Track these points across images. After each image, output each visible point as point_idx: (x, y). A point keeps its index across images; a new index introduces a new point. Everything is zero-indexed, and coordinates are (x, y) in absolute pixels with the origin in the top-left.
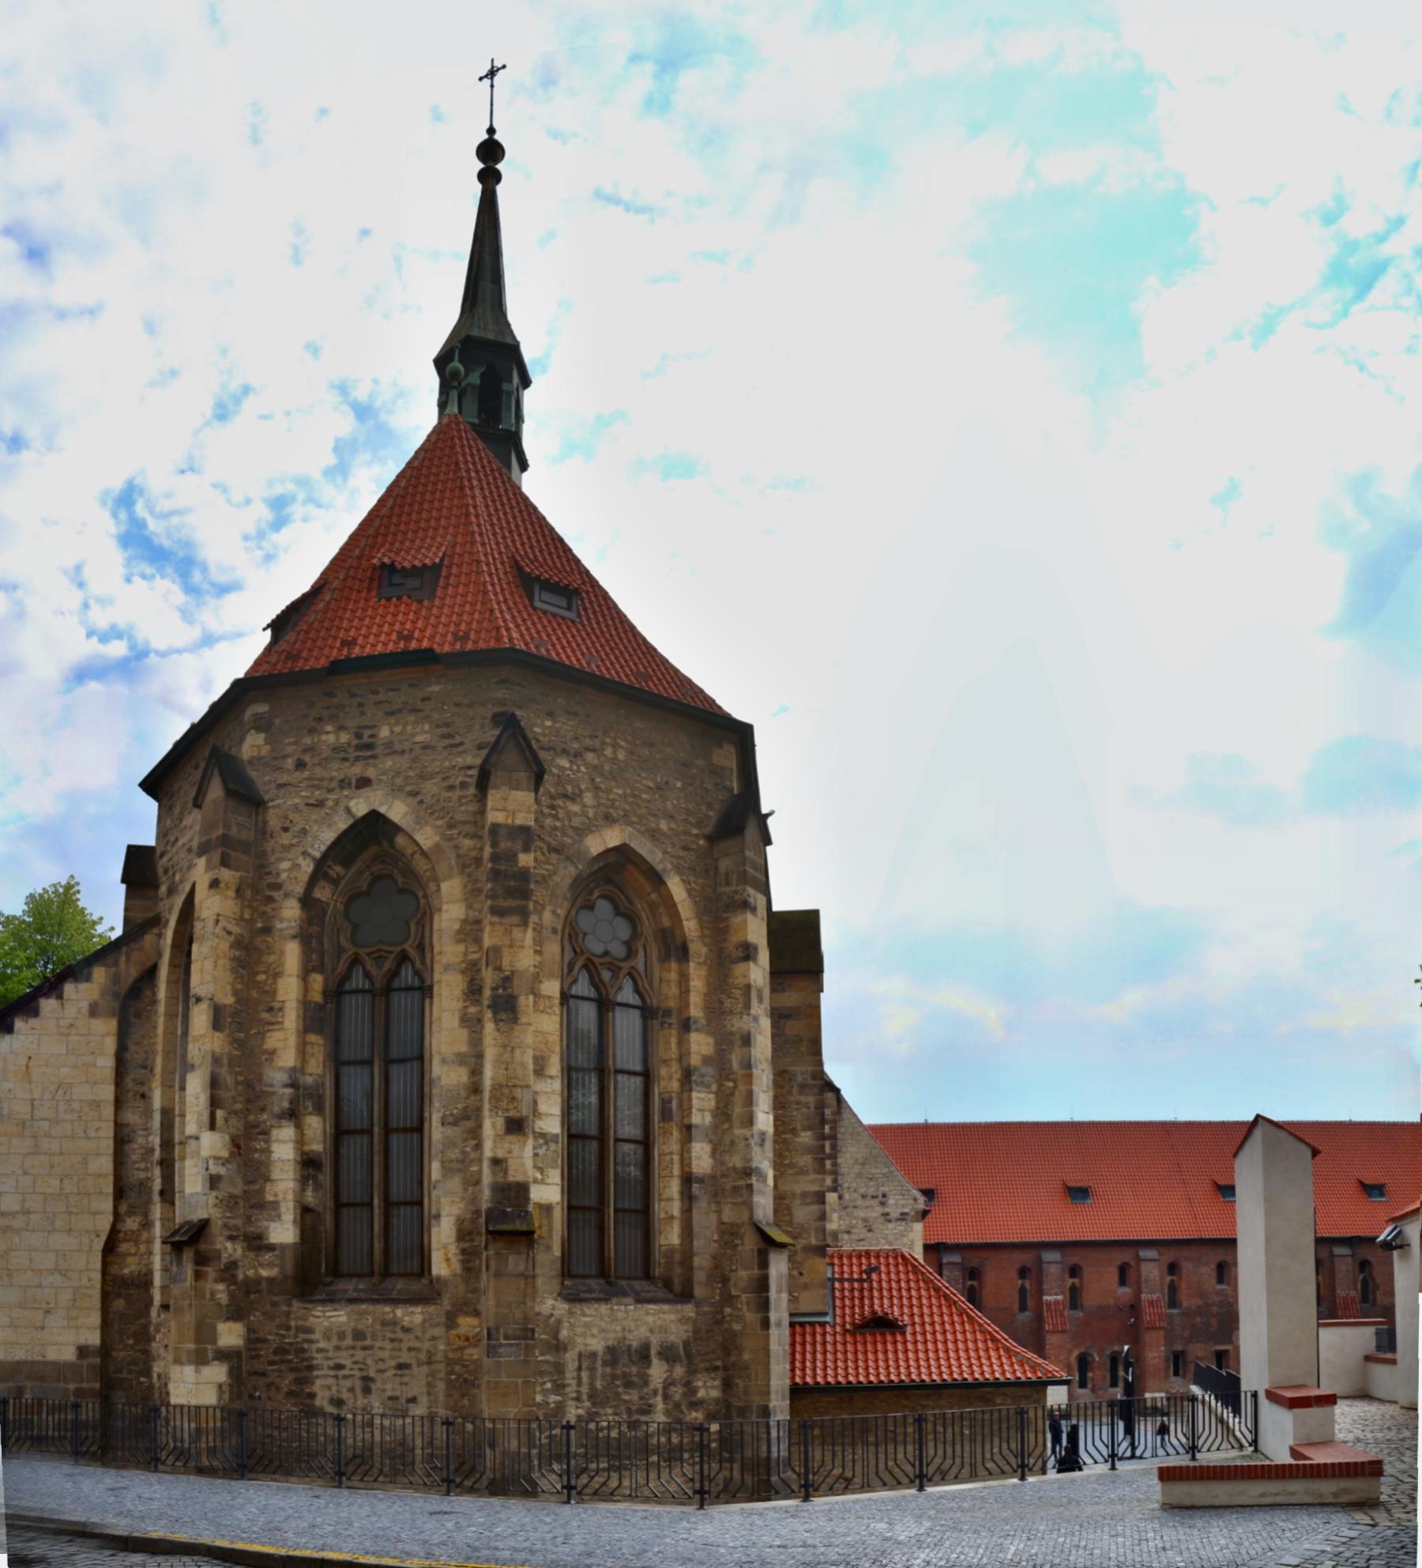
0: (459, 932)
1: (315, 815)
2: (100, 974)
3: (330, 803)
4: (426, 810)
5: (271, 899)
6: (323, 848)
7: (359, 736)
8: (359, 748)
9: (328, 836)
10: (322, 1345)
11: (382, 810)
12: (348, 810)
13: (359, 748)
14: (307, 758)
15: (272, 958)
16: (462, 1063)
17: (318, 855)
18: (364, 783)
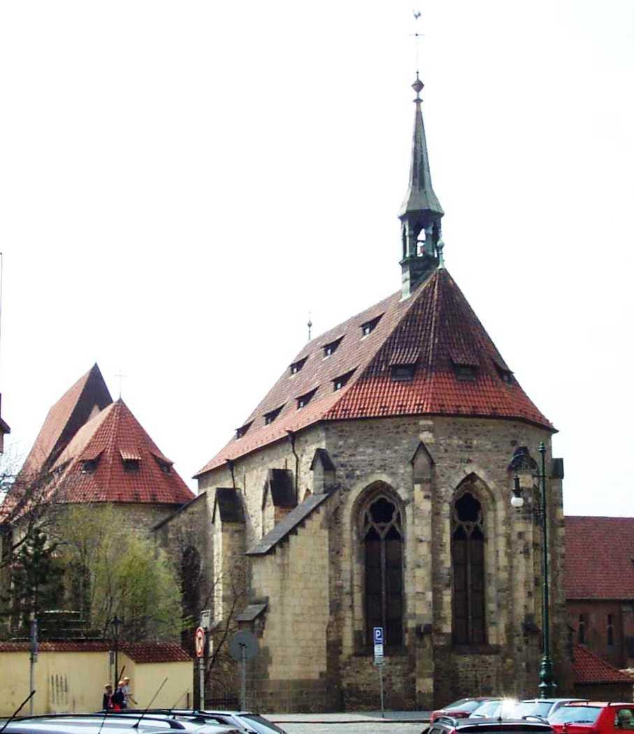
0: (504, 521)
1: (453, 471)
2: (322, 510)
3: (458, 467)
4: (492, 475)
5: (439, 502)
6: (457, 484)
7: (466, 442)
8: (466, 447)
9: (458, 481)
10: (462, 669)
11: (476, 472)
12: (464, 471)
13: (466, 447)
15: (441, 526)
16: (507, 571)
17: (455, 487)
18: (469, 461)
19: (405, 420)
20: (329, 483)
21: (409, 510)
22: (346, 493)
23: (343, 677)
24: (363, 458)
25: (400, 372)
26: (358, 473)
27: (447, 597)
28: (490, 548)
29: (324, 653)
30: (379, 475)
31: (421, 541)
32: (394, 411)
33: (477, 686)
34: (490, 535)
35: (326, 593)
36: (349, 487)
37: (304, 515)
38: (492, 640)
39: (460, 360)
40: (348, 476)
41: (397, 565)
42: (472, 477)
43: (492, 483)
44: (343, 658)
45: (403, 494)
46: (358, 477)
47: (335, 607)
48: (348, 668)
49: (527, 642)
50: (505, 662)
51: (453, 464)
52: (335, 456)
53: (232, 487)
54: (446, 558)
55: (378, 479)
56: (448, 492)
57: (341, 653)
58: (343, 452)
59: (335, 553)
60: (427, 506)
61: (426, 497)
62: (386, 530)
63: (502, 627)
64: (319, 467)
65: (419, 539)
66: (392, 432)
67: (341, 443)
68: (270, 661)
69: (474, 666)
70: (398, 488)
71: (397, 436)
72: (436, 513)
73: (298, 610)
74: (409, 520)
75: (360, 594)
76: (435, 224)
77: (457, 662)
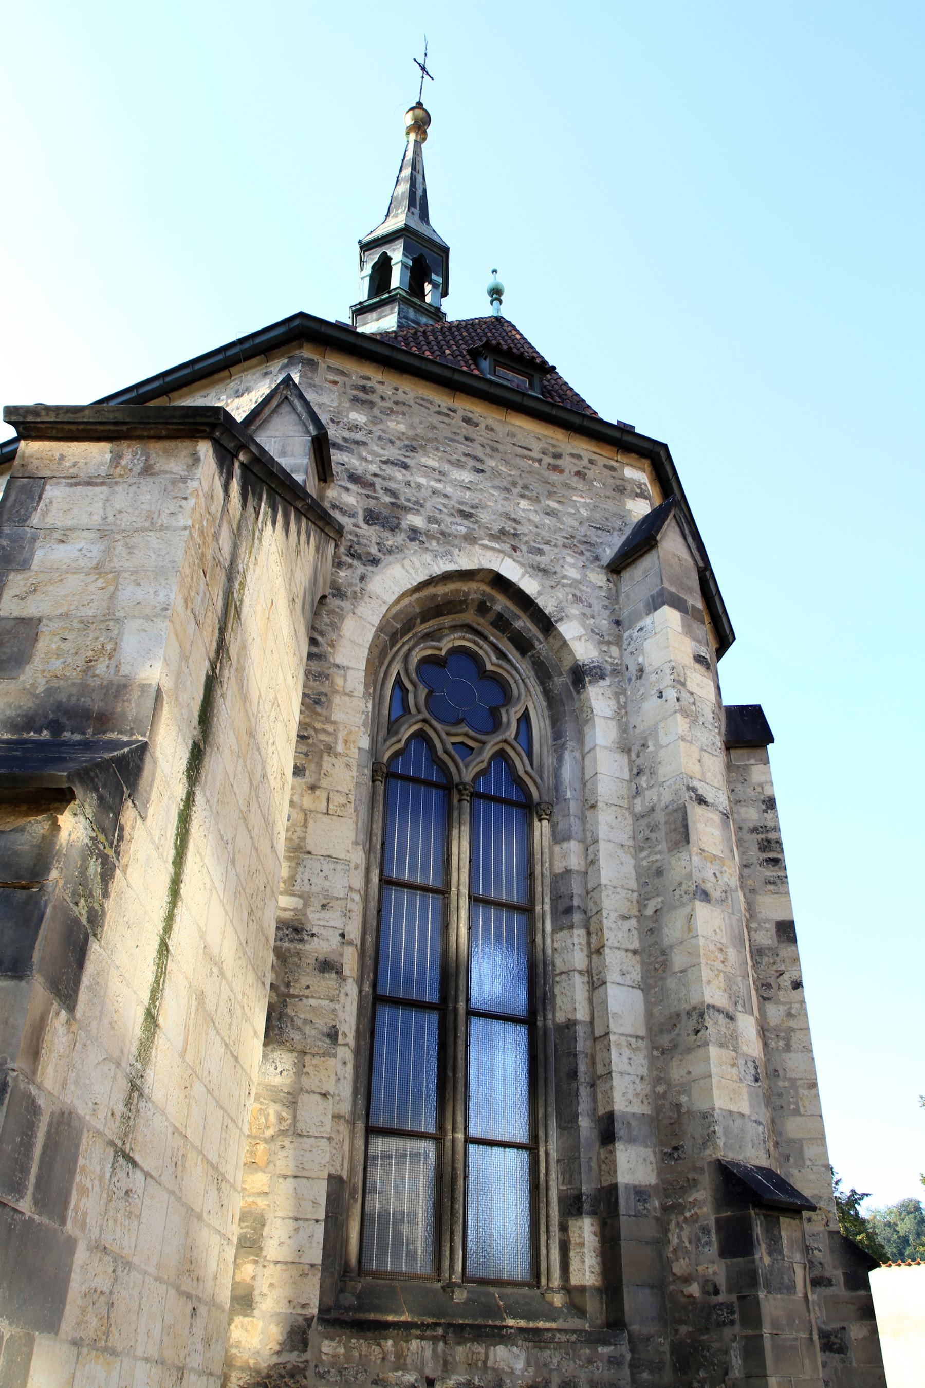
22: (360, 569)
24: (439, 486)
30: (489, 554)
31: (701, 801)
36: (374, 550)
46: (414, 534)
58: (364, 444)
65: (694, 789)
66: (540, 461)
67: (358, 417)
70: (561, 619)
71: (555, 477)
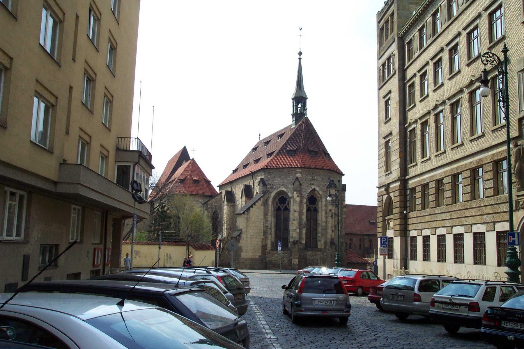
1: (307, 187)
2: (262, 199)
4: (321, 189)
8: (313, 179)
9: (309, 191)
13: (313, 179)
14: (306, 179)
18: (313, 184)
19: (292, 169)
20: (264, 190)
21: (292, 201)
23: (267, 257)
25: (290, 152)
26: (275, 187)
27: (304, 231)
28: (319, 215)
29: (261, 249)
31: (296, 211)
32: (288, 166)
33: (313, 262)
34: (320, 210)
35: (262, 228)
37: (255, 201)
38: (319, 247)
39: (311, 149)
40: (271, 188)
41: (287, 220)
42: (314, 190)
43: (321, 192)
44: (267, 251)
45: (290, 195)
46: (275, 188)
47: (265, 233)
48: (269, 254)
49: (331, 248)
50: (323, 254)
51: (308, 185)
52: (267, 181)
53: (231, 190)
54: (304, 217)
55: (281, 189)
56: (306, 195)
57: (266, 249)
59: (266, 214)
60: (298, 199)
61: (298, 196)
62: (284, 207)
63: (323, 242)
64: (261, 184)
67: (269, 176)
68: (242, 251)
69: (312, 255)
72: (301, 202)
73: (252, 234)
74: (292, 204)
75: (274, 229)
76: (304, 102)
77: (307, 254)
